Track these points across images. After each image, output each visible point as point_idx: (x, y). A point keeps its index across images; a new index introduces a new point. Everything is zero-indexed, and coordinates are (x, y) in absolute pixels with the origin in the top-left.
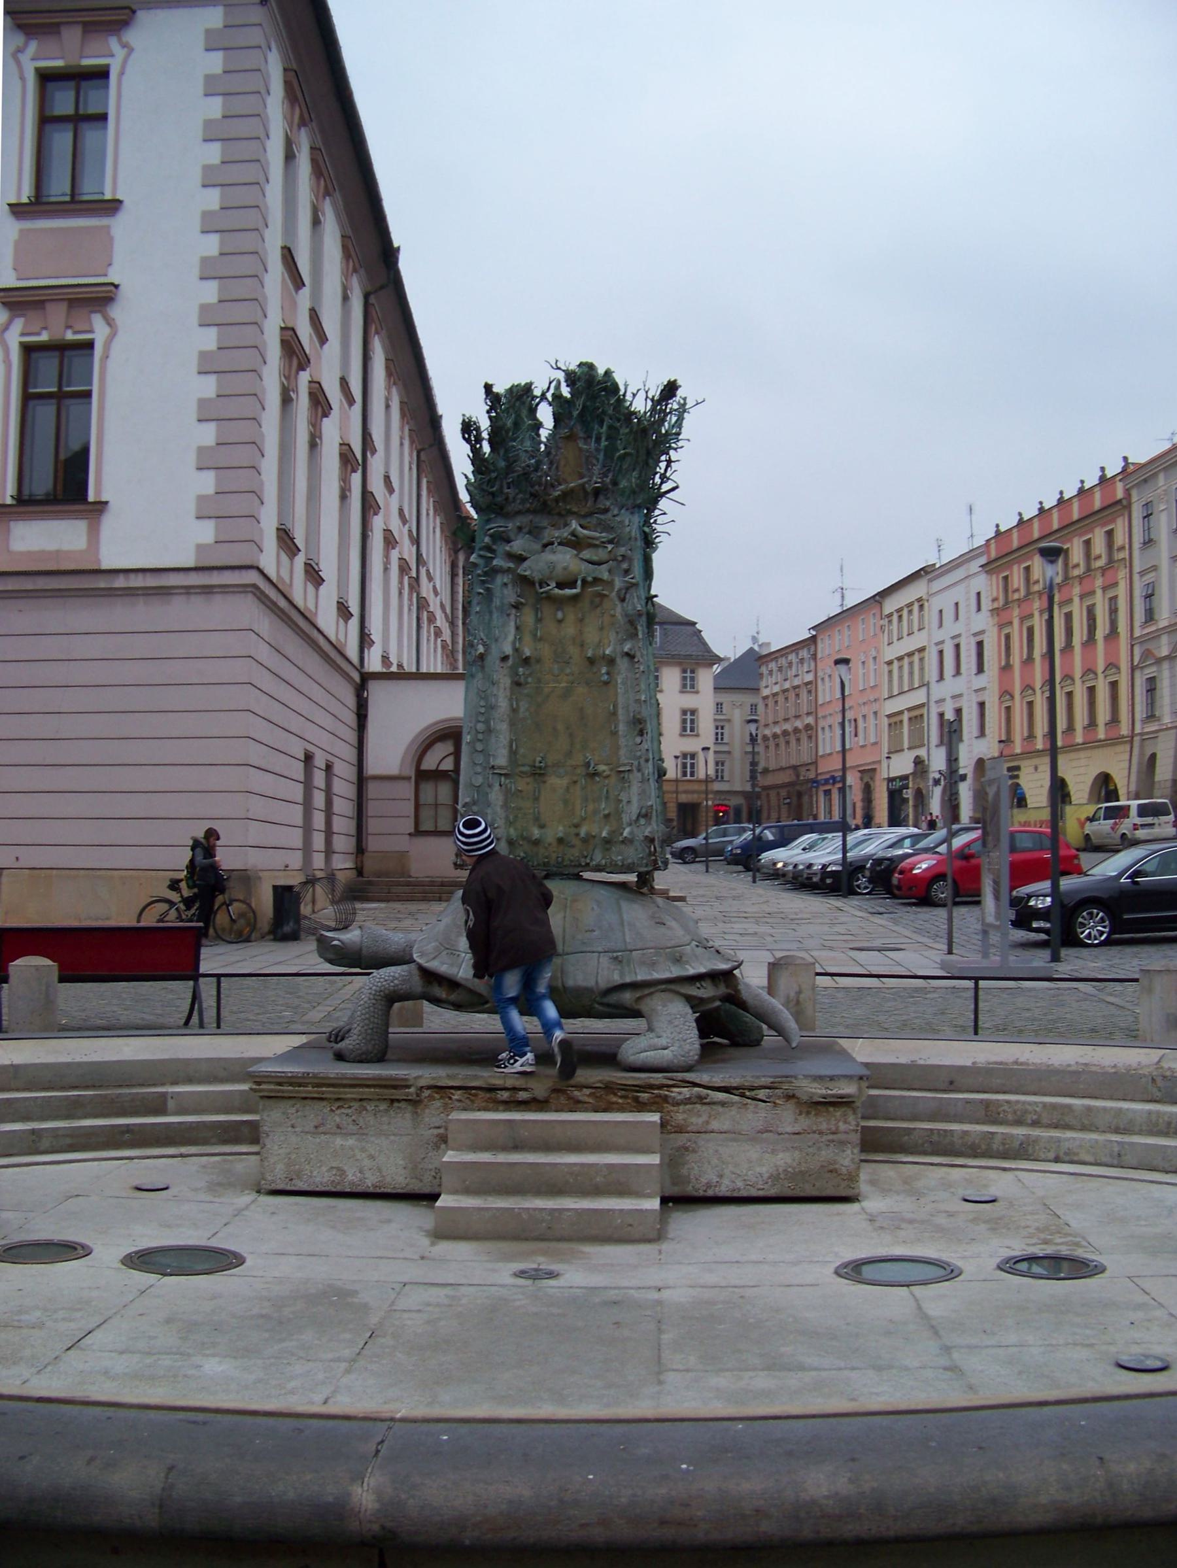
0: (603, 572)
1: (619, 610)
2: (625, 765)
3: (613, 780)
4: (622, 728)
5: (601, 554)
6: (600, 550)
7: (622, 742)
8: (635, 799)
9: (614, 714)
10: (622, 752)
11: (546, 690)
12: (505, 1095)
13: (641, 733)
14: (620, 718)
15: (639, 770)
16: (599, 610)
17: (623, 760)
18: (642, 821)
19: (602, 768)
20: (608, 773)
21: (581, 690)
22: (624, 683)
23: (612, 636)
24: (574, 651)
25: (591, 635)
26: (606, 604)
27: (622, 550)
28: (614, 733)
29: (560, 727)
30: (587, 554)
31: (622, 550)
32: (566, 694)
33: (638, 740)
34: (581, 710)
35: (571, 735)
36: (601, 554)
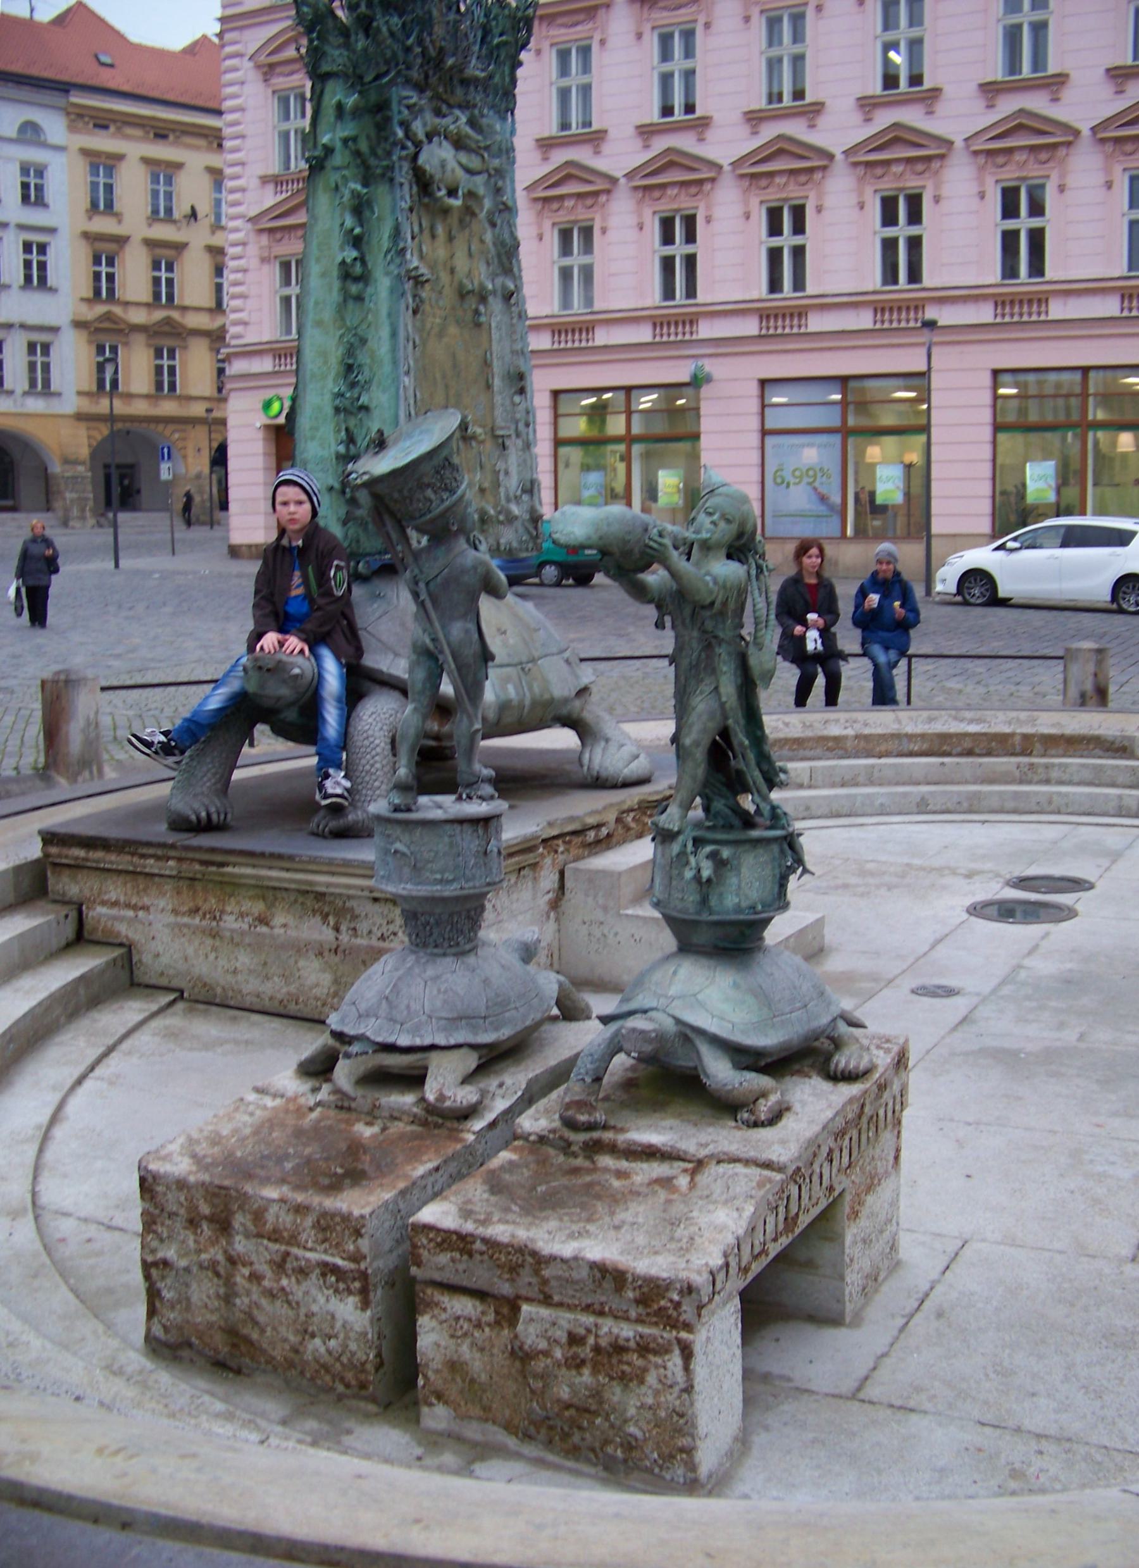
0: (479, 183)
1: (488, 237)
2: (502, 428)
3: (489, 446)
4: (497, 383)
5: (474, 163)
6: (473, 156)
7: (498, 399)
8: (514, 470)
9: (487, 364)
10: (498, 412)
11: (428, 326)
12: (591, 835)
13: (522, 391)
14: (496, 370)
15: (518, 435)
16: (467, 231)
17: (499, 422)
18: (525, 498)
19: (479, 431)
20: (482, 437)
21: (453, 330)
22: (498, 328)
23: (483, 268)
24: (445, 277)
25: (461, 263)
26: (475, 226)
27: (496, 162)
28: (489, 387)
29: (438, 376)
30: (464, 158)
31: (496, 162)
32: (441, 334)
33: (517, 399)
34: (454, 355)
35: (447, 387)
36: (474, 163)
